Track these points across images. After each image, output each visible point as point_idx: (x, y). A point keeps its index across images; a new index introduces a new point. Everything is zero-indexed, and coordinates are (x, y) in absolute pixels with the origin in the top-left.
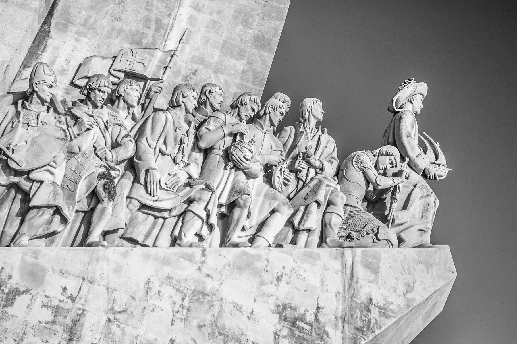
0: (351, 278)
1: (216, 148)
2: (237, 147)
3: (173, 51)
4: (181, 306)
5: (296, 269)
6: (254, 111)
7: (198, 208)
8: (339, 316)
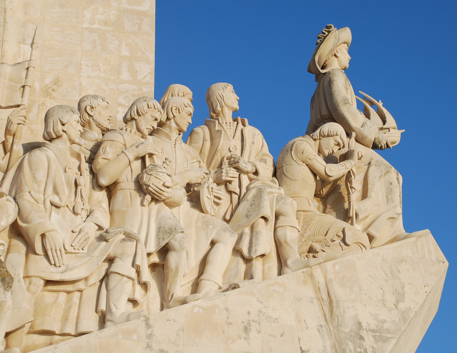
0: (329, 303)
1: (122, 181)
2: (151, 175)
3: (27, 63)
5: (264, 310)
6: (156, 119)
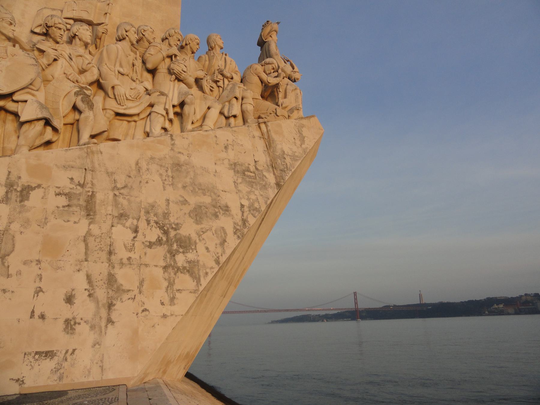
4: (167, 176)
5: (235, 140)
7: (160, 109)
8: (269, 164)
